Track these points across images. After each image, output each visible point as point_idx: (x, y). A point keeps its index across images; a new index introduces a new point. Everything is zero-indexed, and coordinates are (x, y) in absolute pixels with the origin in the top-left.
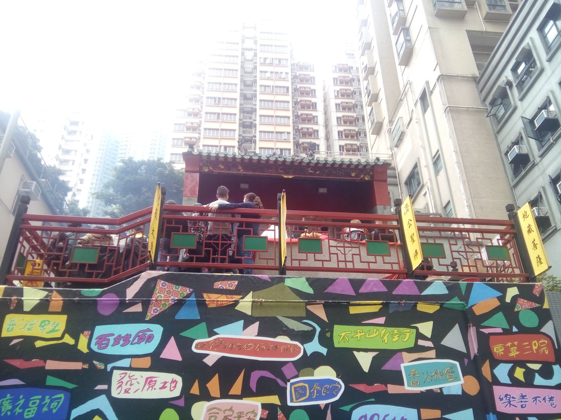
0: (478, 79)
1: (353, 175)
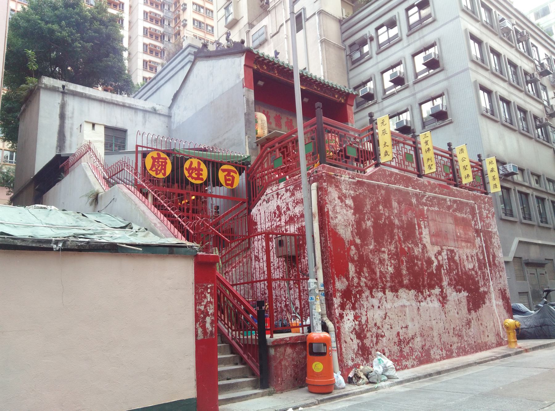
1: (336, 96)
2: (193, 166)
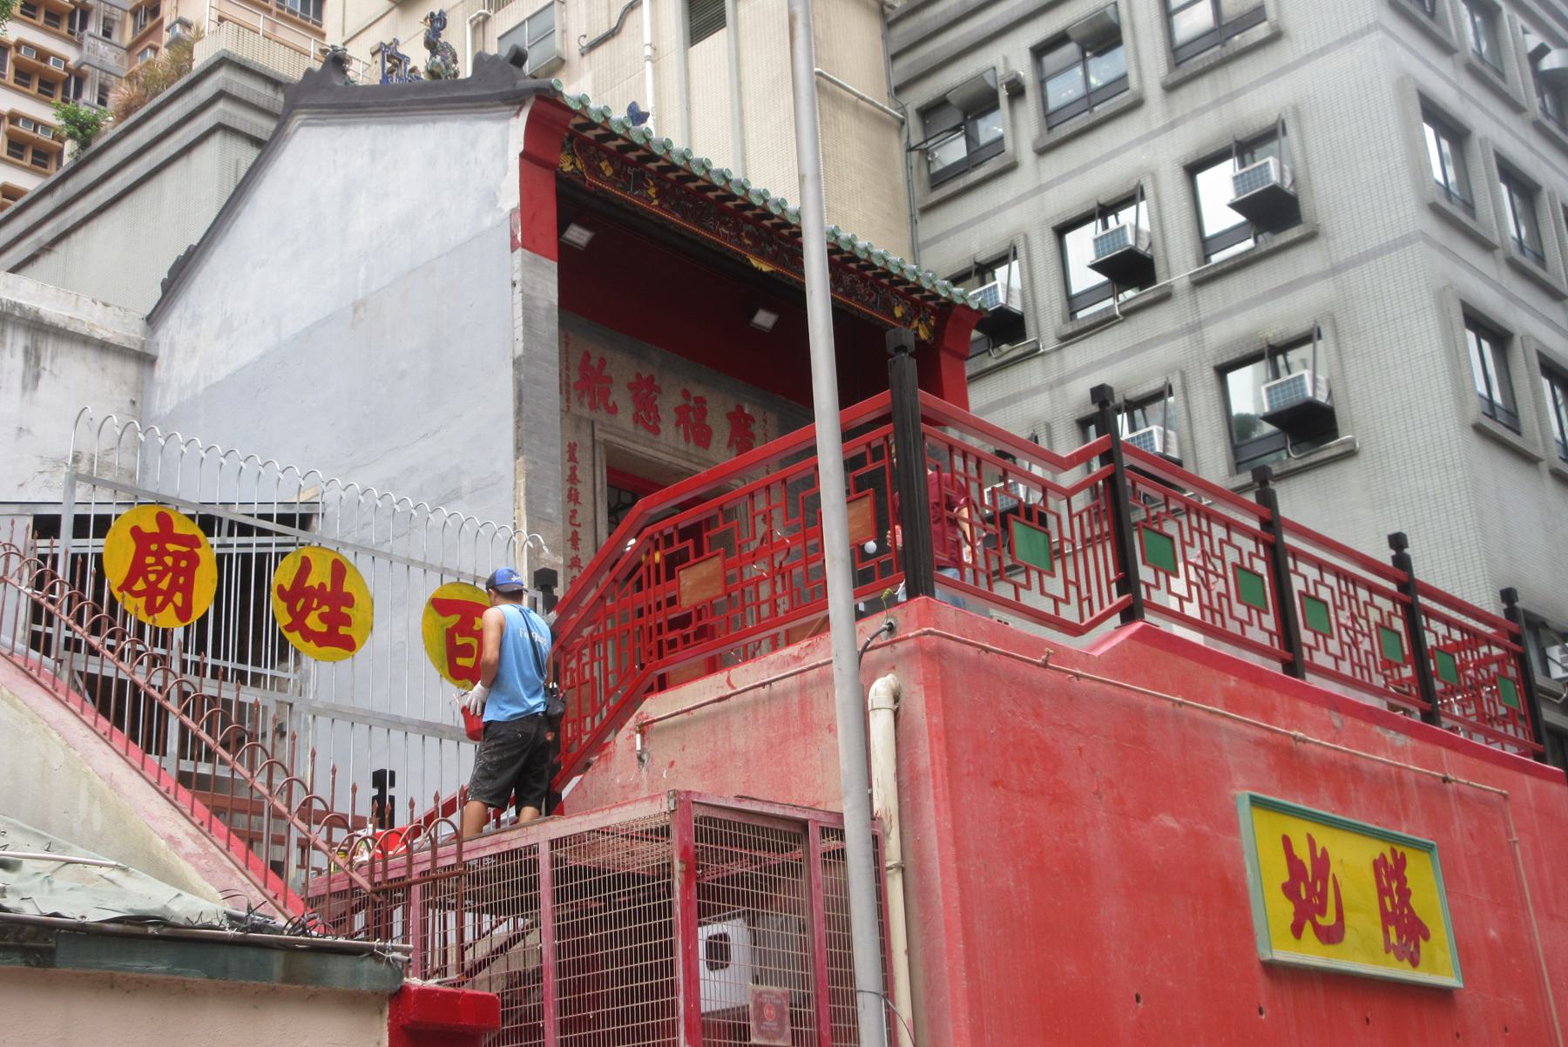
0: (892, 15)
1: (898, 312)
2: (313, 581)
